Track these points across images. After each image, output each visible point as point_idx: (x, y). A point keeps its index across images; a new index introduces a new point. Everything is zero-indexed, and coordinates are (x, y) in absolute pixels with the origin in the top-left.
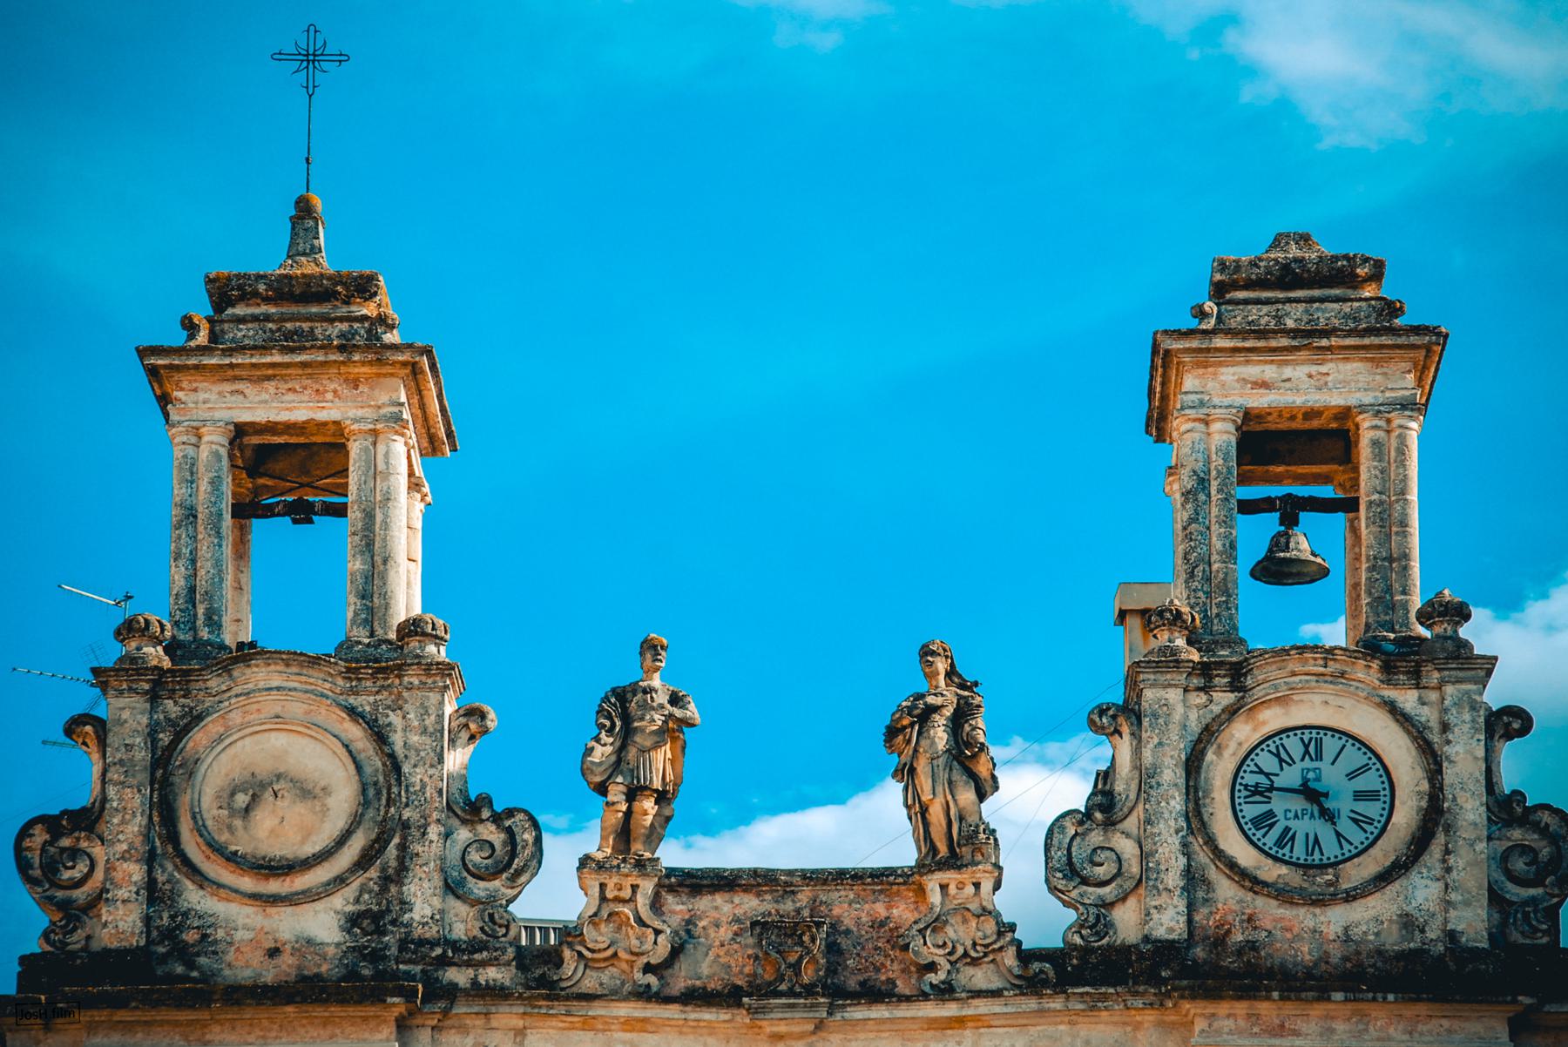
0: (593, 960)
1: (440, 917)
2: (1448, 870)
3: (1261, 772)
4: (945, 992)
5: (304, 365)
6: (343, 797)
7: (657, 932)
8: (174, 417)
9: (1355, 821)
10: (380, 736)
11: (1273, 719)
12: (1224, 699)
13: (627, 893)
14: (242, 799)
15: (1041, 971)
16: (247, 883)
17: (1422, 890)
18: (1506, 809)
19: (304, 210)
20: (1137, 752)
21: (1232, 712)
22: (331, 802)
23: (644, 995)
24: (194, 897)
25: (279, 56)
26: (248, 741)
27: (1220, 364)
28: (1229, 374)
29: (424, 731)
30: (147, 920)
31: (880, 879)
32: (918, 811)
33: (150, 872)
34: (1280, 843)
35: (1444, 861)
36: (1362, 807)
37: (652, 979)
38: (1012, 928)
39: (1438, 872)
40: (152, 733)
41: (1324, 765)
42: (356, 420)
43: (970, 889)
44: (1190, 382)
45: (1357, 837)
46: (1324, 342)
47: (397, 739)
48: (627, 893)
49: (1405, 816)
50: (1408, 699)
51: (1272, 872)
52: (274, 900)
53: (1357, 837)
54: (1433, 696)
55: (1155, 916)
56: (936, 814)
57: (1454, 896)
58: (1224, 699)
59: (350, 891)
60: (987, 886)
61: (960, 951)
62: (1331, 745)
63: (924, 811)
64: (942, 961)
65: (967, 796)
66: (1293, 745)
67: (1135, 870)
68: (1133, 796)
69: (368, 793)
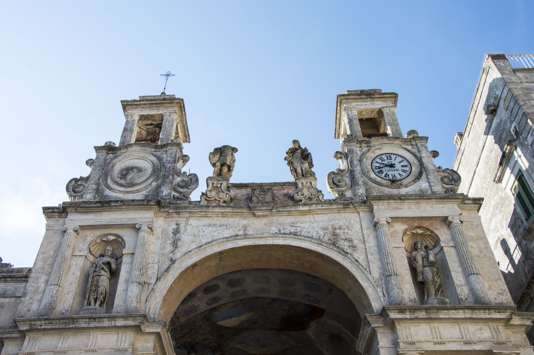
0: (209, 201)
5: (155, 104)
6: (150, 171)
7: (227, 194)
10: (160, 159)
11: (378, 152)
12: (365, 149)
13: (219, 186)
14: (124, 172)
16: (122, 189)
17: (423, 184)
24: (108, 192)
28: (354, 104)
29: (171, 157)
32: (294, 171)
33: (98, 187)
34: (385, 176)
36: (404, 168)
39: (426, 180)
40: (105, 160)
43: (309, 184)
45: (404, 174)
47: (164, 160)
48: (219, 186)
49: (415, 170)
50: (409, 148)
51: (384, 182)
52: (128, 192)
53: (404, 174)
56: (299, 170)
58: (365, 149)
60: (313, 183)
61: (308, 197)
62: (393, 157)
63: (296, 171)
65: (306, 165)
66: (384, 157)
67: (350, 183)
69: (156, 171)
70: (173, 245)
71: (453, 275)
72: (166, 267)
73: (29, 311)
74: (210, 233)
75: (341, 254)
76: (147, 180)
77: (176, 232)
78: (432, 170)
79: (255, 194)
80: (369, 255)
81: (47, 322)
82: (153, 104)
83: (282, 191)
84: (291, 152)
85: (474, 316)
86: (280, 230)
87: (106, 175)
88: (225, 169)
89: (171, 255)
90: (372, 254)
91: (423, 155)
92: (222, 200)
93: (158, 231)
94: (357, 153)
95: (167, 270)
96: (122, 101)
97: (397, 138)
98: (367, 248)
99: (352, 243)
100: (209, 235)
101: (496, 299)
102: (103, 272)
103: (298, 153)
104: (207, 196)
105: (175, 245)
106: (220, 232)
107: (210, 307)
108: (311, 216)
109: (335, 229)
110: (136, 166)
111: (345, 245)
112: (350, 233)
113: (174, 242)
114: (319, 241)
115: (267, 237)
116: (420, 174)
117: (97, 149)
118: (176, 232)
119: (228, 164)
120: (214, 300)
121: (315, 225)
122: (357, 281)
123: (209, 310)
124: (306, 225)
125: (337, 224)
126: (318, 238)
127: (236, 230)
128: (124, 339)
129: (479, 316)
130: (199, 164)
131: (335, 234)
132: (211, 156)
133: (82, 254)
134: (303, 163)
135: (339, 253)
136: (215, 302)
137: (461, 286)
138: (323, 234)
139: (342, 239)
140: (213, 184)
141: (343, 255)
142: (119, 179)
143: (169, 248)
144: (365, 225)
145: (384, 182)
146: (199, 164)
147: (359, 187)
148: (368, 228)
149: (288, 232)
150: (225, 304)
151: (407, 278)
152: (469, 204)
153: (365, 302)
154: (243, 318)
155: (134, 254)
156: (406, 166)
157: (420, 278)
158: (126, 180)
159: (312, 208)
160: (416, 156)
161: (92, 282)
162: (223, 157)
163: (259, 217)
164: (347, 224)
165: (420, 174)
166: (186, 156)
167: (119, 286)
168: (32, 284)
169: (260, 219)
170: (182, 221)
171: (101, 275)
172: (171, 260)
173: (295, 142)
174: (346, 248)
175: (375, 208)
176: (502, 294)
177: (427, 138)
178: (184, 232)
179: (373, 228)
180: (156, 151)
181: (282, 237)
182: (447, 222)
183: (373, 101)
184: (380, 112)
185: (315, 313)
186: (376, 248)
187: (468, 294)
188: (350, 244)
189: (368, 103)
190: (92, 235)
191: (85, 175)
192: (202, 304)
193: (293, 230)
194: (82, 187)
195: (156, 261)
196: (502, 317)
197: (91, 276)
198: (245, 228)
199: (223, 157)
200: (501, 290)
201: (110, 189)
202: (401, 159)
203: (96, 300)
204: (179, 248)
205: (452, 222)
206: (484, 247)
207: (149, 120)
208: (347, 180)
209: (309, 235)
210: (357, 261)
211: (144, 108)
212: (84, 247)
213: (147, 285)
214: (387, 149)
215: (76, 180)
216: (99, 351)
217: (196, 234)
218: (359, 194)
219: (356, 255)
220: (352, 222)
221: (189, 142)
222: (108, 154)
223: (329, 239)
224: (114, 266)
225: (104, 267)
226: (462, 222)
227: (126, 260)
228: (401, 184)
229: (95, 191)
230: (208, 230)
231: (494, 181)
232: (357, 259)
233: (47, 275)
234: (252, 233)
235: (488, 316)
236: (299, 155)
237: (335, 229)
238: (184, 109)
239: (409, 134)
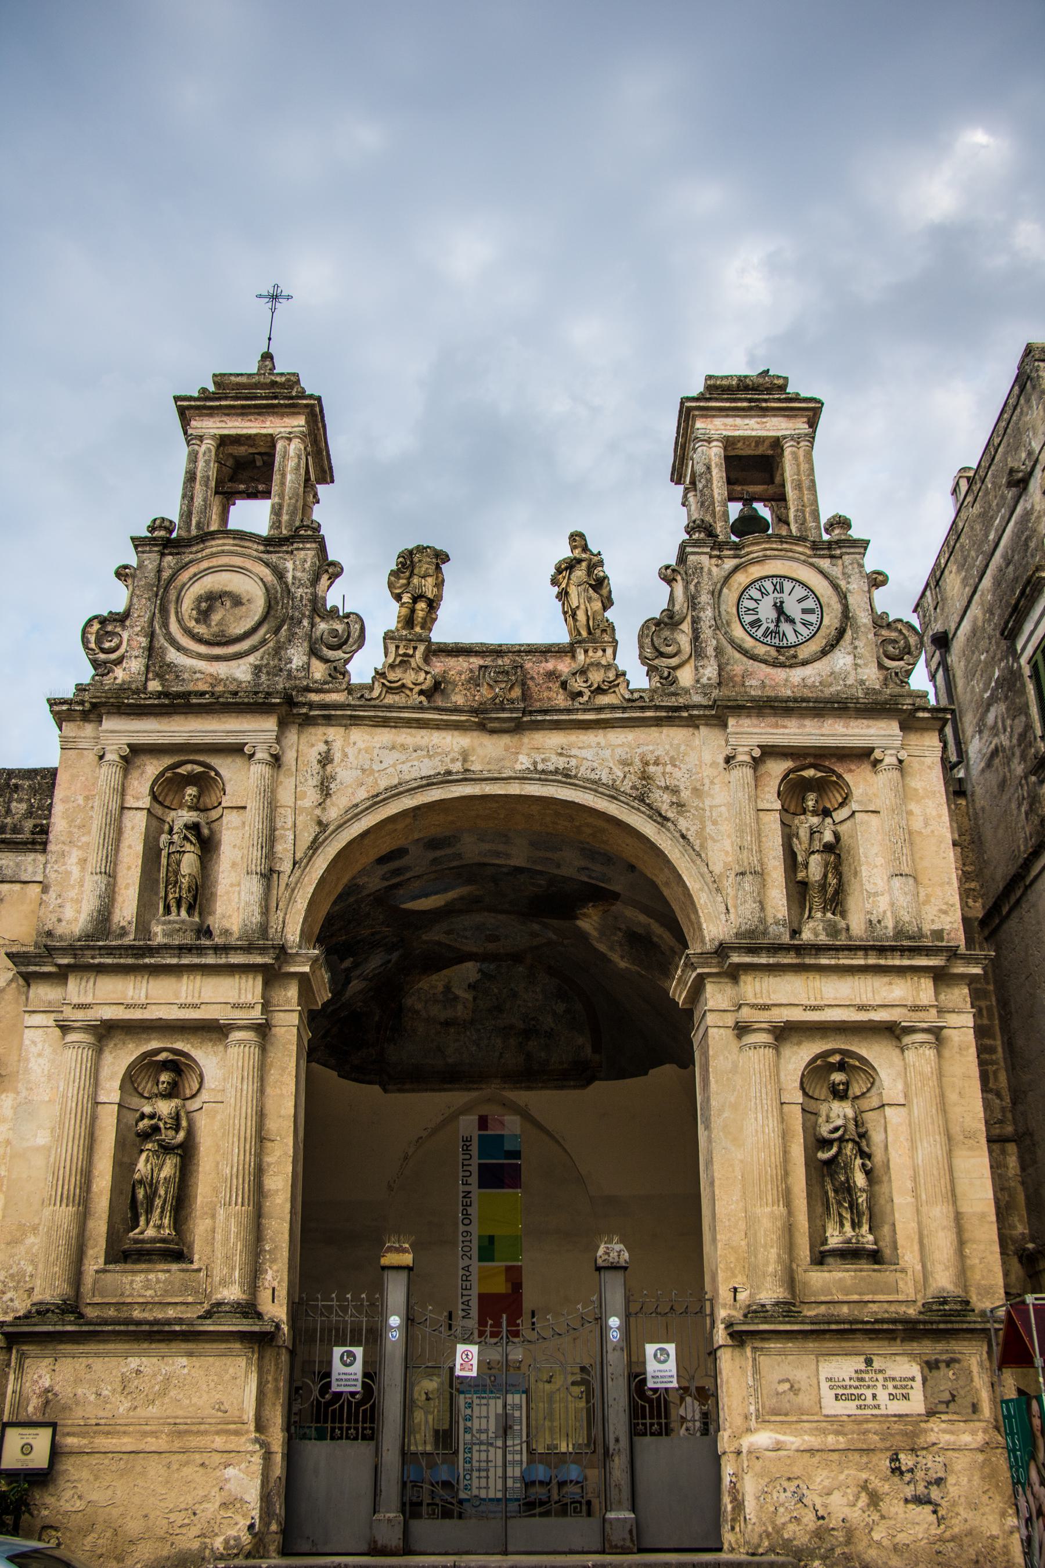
0: (391, 688)
1: (307, 668)
2: (856, 648)
3: (752, 599)
5: (256, 406)
7: (427, 673)
8: (190, 431)
9: (804, 624)
10: (280, 574)
14: (204, 605)
15: (641, 697)
16: (203, 649)
17: (841, 660)
18: (880, 622)
19: (267, 356)
20: (686, 588)
21: (736, 569)
22: (252, 606)
24: (173, 655)
25: (260, 296)
26: (210, 576)
27: (714, 416)
28: (718, 422)
29: (304, 570)
30: (147, 667)
32: (570, 614)
33: (151, 642)
35: (852, 643)
37: (423, 698)
38: (624, 674)
40: (159, 571)
41: (785, 596)
42: (280, 433)
43: (600, 653)
44: (699, 424)
45: (805, 632)
46: (764, 405)
48: (411, 652)
49: (831, 620)
51: (761, 650)
52: (217, 658)
53: (805, 632)
54: (840, 562)
55: (701, 670)
56: (581, 616)
57: (859, 661)
58: (729, 564)
59: (258, 654)
61: (596, 686)
62: (788, 585)
63: (574, 615)
64: (586, 690)
65: (597, 605)
66: (768, 585)
68: (685, 611)
70: (322, 790)
71: (864, 871)
72: (311, 839)
73: (60, 920)
74: (394, 765)
75: (655, 821)
76: (254, 630)
77: (325, 760)
78: (865, 625)
79: (488, 679)
80: (708, 823)
81: (103, 952)
82: (249, 406)
83: (543, 665)
84: (566, 569)
85: (882, 962)
86: (535, 763)
87: (164, 611)
88: (422, 605)
89: (318, 812)
90: (715, 823)
91: (851, 587)
92: (417, 689)
93: (289, 757)
94: (710, 572)
95: (315, 846)
96: (177, 399)
97: (802, 539)
98: (707, 808)
99: (679, 797)
100: (391, 770)
101: (933, 921)
102: (188, 847)
104: (385, 678)
105: (325, 789)
106: (415, 763)
107: (387, 884)
108: (600, 731)
109: (647, 764)
110: (227, 589)
111: (662, 800)
112: (677, 773)
113: (322, 784)
114: (614, 794)
115: (510, 778)
116: (841, 633)
117: (138, 543)
118: (325, 760)
119: (430, 596)
120: (397, 872)
121: (607, 753)
122: (680, 876)
123: (386, 888)
125: (652, 752)
126: (610, 783)
127: (448, 760)
128: (243, 985)
129: (890, 962)
131: (645, 777)
132: (393, 578)
133: (140, 804)
134: (590, 599)
135: (650, 817)
136: (399, 875)
137: (876, 894)
138: (622, 775)
139: (659, 787)
140: (397, 647)
141: (659, 823)
142: (192, 624)
143: (312, 796)
144: (707, 757)
146: (365, 595)
147: (705, 662)
148: (714, 764)
149: (552, 768)
150: (418, 877)
151: (775, 876)
152: (923, 718)
153: (693, 917)
154: (451, 895)
155: (244, 808)
156: (810, 611)
157: (801, 875)
158: (209, 626)
159: (603, 716)
160: (836, 587)
161: (168, 865)
162: (418, 574)
163: (493, 732)
164: (672, 753)
165: (841, 633)
166: (333, 564)
167: (221, 876)
168: (56, 867)
169: (495, 736)
171: (184, 852)
172: (320, 823)
173: (577, 539)
174: (665, 808)
175: (731, 722)
176: (945, 912)
177: (868, 542)
178: (342, 761)
179: (722, 764)
180: (269, 552)
181: (540, 779)
182: (872, 758)
183: (764, 416)
184: (777, 444)
185: (600, 895)
186: (723, 809)
187: (885, 912)
188: (674, 800)
189: (752, 422)
190: (155, 762)
191: (120, 608)
192: (374, 883)
193: (561, 763)
194: (116, 641)
195: (290, 824)
196: (931, 963)
197: (164, 853)
198: (465, 756)
199: (418, 574)
200: (947, 904)
201: (179, 648)
202: (803, 592)
203: (179, 902)
204: (334, 798)
205: (881, 761)
206: (934, 813)
207: (241, 445)
208: (684, 639)
209: (593, 776)
210: (683, 837)
211: (228, 415)
212: (142, 790)
213: (275, 876)
215: (103, 621)
216: (202, 1006)
217: (366, 767)
218: (704, 680)
219: (683, 824)
220: (683, 748)
221: (332, 481)
222: (163, 555)
223: (634, 787)
224: (206, 831)
225: (189, 836)
226: (901, 761)
227: (231, 819)
228: (795, 657)
229: (146, 653)
231: (1002, 634)
232: (684, 832)
233: (80, 848)
234: (479, 768)
235: (906, 962)
237: (647, 764)
238: (323, 417)
239: (830, 526)
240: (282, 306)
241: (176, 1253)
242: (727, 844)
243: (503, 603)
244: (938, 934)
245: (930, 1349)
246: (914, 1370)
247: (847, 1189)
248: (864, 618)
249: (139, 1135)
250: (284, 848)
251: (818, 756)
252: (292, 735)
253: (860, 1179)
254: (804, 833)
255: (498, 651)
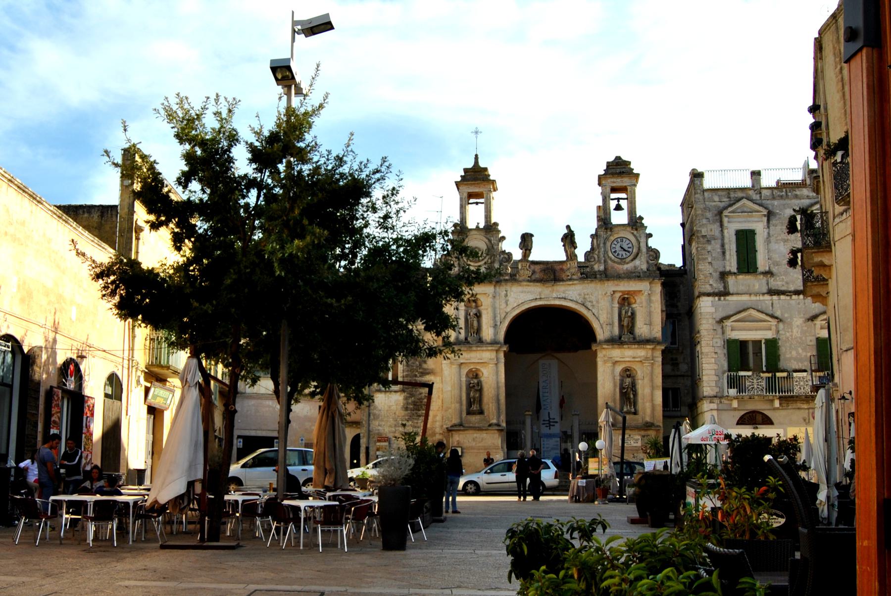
4: (570, 280)
10: (490, 241)
11: (616, 236)
12: (609, 233)
17: (637, 262)
19: (476, 156)
23: (528, 281)
28: (609, 180)
31: (561, 263)
32: (566, 251)
49: (635, 250)
51: (616, 260)
103: (568, 240)
111: (589, 305)
116: (637, 254)
118: (506, 295)
124: (570, 293)
130: (511, 246)
131: (584, 298)
143: (503, 305)
145: (616, 260)
162: (526, 241)
165: (637, 254)
170: (508, 288)
173: (568, 227)
189: (619, 180)
199: (526, 241)
208: (596, 256)
214: (622, 234)
230: (522, 295)
236: (569, 239)
240: (479, 135)
241: (481, 412)
242: (605, 316)
243: (549, 250)
244: (655, 338)
245: (643, 433)
246: (640, 437)
247: (629, 398)
248: (644, 249)
249: (470, 387)
250: (498, 319)
251: (628, 293)
252: (497, 288)
253: (632, 396)
254: (623, 312)
255: (547, 263)
